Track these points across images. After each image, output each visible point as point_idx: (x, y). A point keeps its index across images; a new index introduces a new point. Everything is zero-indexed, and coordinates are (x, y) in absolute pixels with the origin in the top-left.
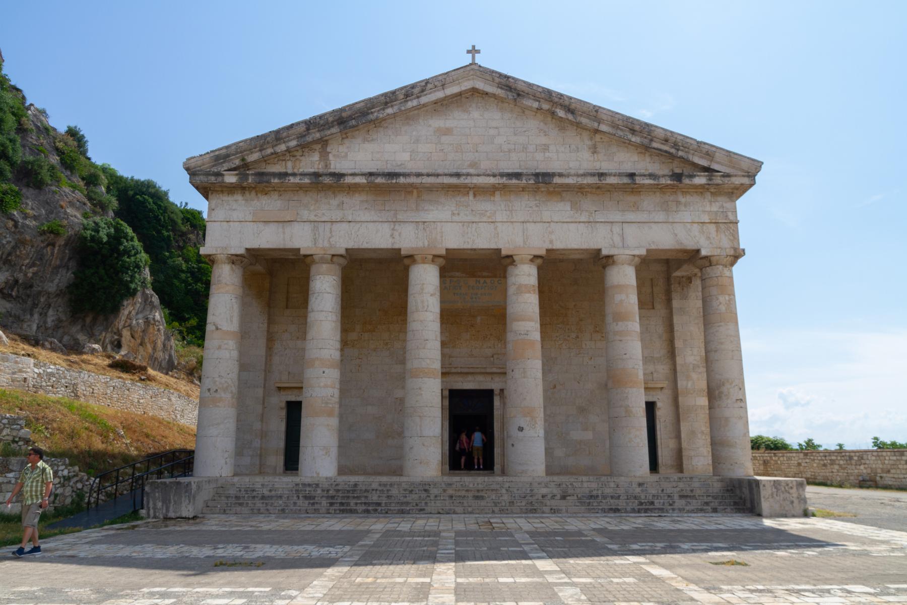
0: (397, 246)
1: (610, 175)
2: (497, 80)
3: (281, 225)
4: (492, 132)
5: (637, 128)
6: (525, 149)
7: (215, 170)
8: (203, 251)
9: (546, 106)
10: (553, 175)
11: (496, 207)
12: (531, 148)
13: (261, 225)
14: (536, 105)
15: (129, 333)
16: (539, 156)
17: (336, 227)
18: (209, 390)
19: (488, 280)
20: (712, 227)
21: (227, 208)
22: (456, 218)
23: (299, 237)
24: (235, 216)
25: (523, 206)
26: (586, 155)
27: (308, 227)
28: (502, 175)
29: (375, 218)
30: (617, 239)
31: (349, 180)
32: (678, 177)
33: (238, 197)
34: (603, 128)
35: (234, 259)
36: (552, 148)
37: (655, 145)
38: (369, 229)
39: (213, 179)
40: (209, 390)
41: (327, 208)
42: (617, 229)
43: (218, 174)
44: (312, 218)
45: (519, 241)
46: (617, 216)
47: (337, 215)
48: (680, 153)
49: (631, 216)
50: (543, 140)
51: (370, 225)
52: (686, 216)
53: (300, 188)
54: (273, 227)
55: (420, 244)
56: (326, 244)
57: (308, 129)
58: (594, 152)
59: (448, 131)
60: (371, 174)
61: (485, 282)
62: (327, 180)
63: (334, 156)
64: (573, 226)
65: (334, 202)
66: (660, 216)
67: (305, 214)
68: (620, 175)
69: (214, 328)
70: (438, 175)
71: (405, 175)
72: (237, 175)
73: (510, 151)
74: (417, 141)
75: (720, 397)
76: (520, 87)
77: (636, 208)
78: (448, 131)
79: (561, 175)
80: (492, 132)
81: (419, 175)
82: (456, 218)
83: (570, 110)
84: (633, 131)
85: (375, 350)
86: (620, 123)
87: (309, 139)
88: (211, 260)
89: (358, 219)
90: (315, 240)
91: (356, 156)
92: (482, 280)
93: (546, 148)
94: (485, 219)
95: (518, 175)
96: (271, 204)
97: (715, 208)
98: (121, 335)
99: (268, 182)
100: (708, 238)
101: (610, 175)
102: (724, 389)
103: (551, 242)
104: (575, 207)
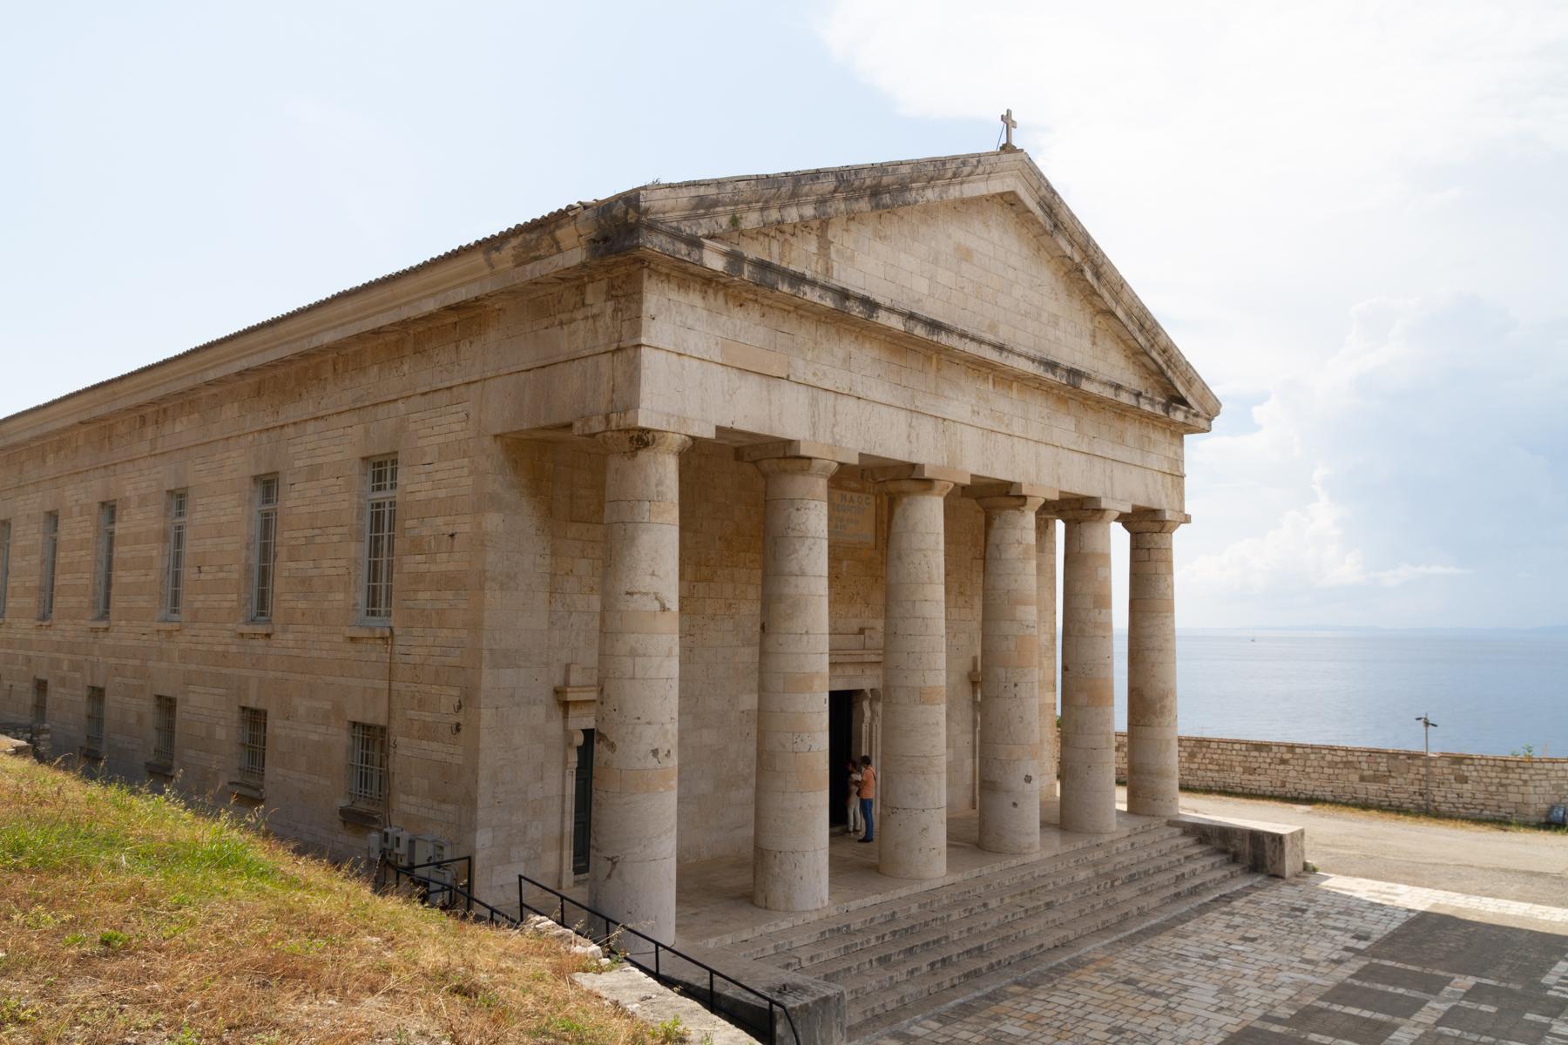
0: (914, 460)
2: (1043, 192)
3: (764, 380)
4: (1011, 274)
5: (1148, 325)
7: (687, 228)
13: (734, 374)
18: (655, 752)
19: (855, 496)
21: (678, 320)
22: (977, 421)
24: (696, 342)
27: (803, 395)
29: (891, 400)
33: (695, 298)
34: (1120, 313)
36: (1062, 323)
37: (1154, 354)
39: (683, 249)
40: (655, 752)
43: (695, 243)
44: (812, 380)
51: (884, 409)
53: (803, 311)
54: (752, 384)
58: (1094, 343)
60: (911, 316)
61: (851, 500)
62: (856, 310)
63: (838, 251)
65: (840, 352)
69: (657, 605)
70: (981, 342)
71: (949, 331)
72: (726, 254)
75: (1162, 713)
76: (1063, 216)
77: (1121, 440)
81: (963, 335)
83: (1098, 275)
84: (1142, 327)
85: (713, 618)
86: (1135, 311)
89: (871, 397)
91: (873, 263)
92: (849, 495)
95: (1052, 366)
99: (773, 288)
102: (1167, 702)
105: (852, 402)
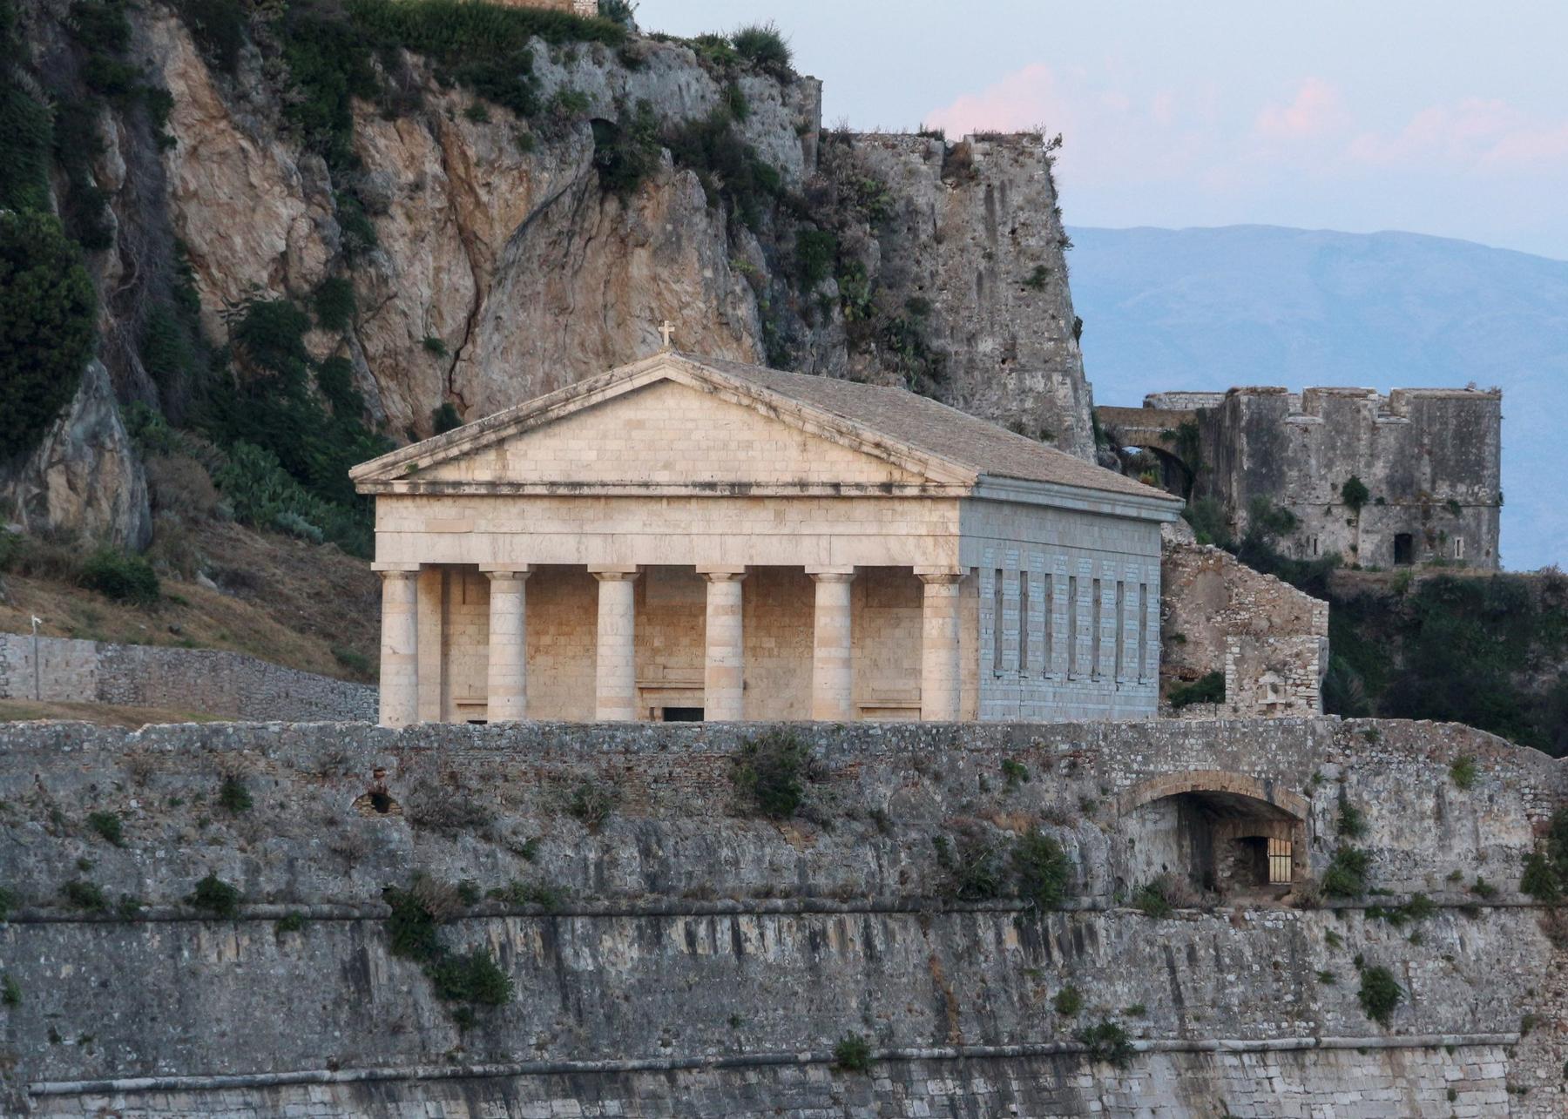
0: (583, 562)
1: (813, 485)
4: (690, 425)
6: (725, 446)
7: (383, 477)
8: (374, 567)
9: (746, 401)
10: (750, 485)
11: (690, 517)
12: (733, 445)
14: (734, 399)
15: (62, 480)
16: (742, 455)
17: (517, 539)
20: (930, 541)
22: (648, 530)
23: (475, 551)
24: (408, 525)
25: (723, 515)
26: (794, 453)
27: (486, 539)
28: (695, 485)
30: (824, 555)
31: (528, 490)
32: (887, 487)
35: (408, 576)
36: (757, 445)
37: (865, 449)
38: (551, 539)
41: (507, 515)
42: (824, 542)
43: (386, 483)
45: (716, 556)
46: (824, 528)
47: (516, 526)
48: (892, 459)
49: (840, 528)
50: (746, 435)
51: (555, 537)
52: (901, 528)
54: (448, 539)
55: (608, 561)
56: (507, 561)
57: (482, 431)
59: (640, 425)
60: (553, 484)
64: (775, 540)
66: (872, 529)
67: (483, 525)
68: (823, 484)
71: (589, 485)
73: (708, 449)
74: (604, 437)
78: (640, 425)
79: (758, 485)
80: (690, 425)
82: (648, 530)
85: (574, 657)
87: (484, 441)
88: (379, 577)
89: (541, 530)
90: (495, 554)
93: (749, 445)
94: (679, 531)
96: (443, 510)
97: (935, 517)
98: (45, 486)
100: (924, 553)
101: (813, 485)
103: (751, 558)
104: (780, 517)
105: (526, 538)
